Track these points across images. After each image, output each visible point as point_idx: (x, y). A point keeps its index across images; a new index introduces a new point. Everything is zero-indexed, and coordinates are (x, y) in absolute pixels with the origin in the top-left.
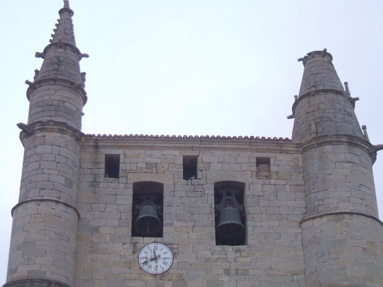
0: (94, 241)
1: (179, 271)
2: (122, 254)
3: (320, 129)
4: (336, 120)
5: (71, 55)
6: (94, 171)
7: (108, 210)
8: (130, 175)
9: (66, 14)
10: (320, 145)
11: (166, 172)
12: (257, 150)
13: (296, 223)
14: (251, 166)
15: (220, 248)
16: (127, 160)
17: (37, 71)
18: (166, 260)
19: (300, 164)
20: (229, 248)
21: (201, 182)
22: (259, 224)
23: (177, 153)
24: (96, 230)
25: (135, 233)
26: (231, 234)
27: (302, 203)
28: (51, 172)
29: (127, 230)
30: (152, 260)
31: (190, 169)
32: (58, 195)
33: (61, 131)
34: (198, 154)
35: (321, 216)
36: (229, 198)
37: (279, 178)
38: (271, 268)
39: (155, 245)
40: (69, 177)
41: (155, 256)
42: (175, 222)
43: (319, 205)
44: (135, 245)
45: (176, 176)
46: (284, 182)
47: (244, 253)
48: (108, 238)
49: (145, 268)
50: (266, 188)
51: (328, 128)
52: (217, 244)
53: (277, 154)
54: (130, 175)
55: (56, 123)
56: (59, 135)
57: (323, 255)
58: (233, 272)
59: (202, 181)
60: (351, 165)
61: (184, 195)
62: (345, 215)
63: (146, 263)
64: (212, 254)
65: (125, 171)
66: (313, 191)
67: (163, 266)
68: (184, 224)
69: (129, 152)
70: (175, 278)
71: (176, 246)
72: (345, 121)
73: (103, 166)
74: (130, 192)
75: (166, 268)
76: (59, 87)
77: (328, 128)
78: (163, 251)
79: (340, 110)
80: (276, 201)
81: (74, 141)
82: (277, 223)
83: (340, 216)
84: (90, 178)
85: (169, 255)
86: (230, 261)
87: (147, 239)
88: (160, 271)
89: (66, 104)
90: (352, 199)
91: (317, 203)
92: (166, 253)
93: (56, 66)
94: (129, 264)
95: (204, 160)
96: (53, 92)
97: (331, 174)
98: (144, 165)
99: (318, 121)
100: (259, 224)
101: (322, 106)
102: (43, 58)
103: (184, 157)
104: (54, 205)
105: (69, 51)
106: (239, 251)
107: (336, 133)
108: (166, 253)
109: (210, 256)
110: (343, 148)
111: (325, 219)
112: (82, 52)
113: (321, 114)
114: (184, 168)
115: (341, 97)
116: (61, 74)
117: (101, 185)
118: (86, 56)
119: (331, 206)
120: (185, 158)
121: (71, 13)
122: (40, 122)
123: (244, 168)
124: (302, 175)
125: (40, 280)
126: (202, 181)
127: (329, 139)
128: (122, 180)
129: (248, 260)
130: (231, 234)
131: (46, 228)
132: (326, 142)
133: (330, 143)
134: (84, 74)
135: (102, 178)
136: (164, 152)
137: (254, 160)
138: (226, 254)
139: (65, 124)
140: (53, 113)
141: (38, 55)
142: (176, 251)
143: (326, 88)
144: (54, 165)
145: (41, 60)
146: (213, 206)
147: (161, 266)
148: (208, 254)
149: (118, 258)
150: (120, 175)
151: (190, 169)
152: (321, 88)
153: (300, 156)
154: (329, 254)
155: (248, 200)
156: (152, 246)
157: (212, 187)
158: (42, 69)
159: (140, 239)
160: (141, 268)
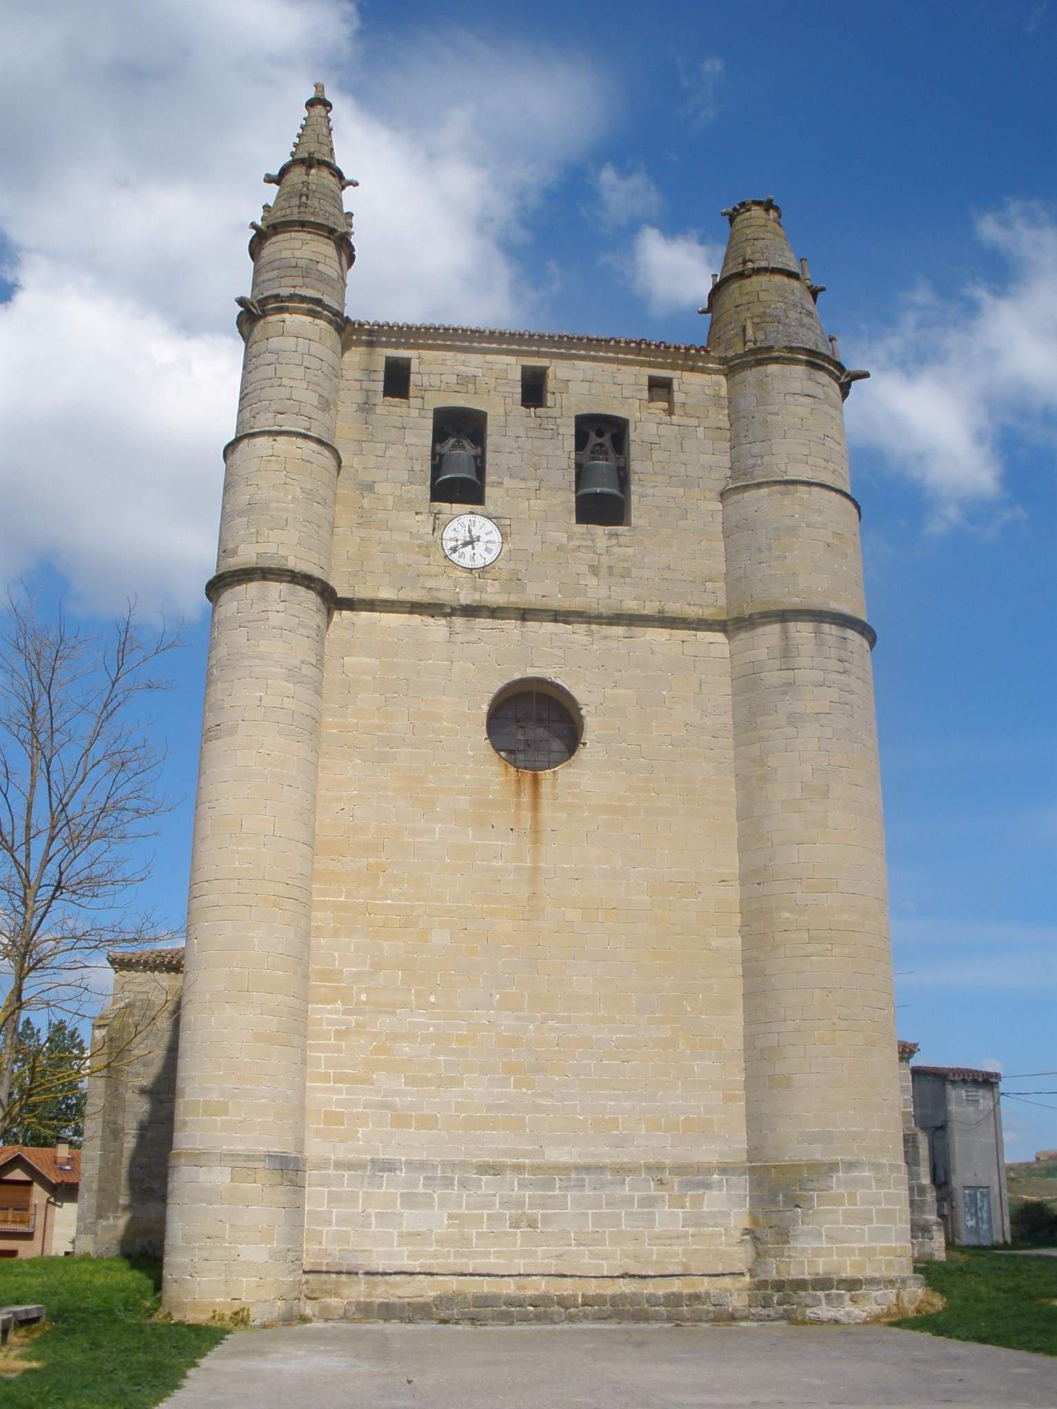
0: (366, 506)
1: (511, 565)
2: (414, 530)
3: (760, 336)
4: (787, 321)
5: (332, 181)
6: (365, 385)
7: (390, 452)
8: (428, 395)
9: (319, 109)
10: (760, 363)
11: (492, 392)
13: (713, 494)
14: (641, 390)
15: (583, 528)
16: (423, 368)
17: (266, 207)
18: (489, 545)
20: (600, 530)
21: (551, 412)
22: (650, 491)
23: (511, 360)
24: (369, 487)
25: (435, 498)
26: (602, 506)
27: (725, 460)
28: (292, 383)
29: (424, 490)
30: (465, 544)
31: (534, 390)
32: (307, 425)
33: (311, 313)
34: (547, 364)
35: (759, 485)
36: (600, 441)
37: (686, 415)
38: (669, 568)
39: (471, 517)
40: (325, 393)
41: (471, 537)
42: (506, 480)
43: (755, 465)
44: (436, 516)
45: (509, 401)
46: (695, 422)
47: (622, 540)
49: (454, 557)
50: (664, 430)
51: (774, 335)
52: (579, 521)
53: (685, 373)
54: (428, 395)
55: (303, 299)
56: (309, 319)
57: (760, 550)
59: (555, 412)
60: (810, 400)
61: (522, 433)
62: (799, 487)
63: (454, 550)
64: (570, 538)
65: (421, 387)
66: (744, 441)
67: (485, 554)
68: (523, 485)
70: (504, 576)
72: (803, 325)
73: (381, 376)
74: (429, 423)
75: (490, 558)
76: (309, 236)
77: (774, 335)
78: (485, 529)
79: (795, 305)
80: (681, 454)
81: (333, 331)
82: (681, 491)
83: (791, 487)
84: (360, 399)
85: (496, 536)
86: (599, 552)
87: (456, 507)
88: (479, 563)
89: (321, 267)
90: (811, 460)
91: (751, 461)
92: (491, 532)
93: (304, 199)
95: (559, 375)
96: (298, 245)
97: (777, 414)
98: (454, 379)
99: (757, 320)
100: (650, 491)
101: (764, 296)
102: (278, 183)
103: (524, 368)
104: (299, 441)
105: (325, 173)
107: (786, 344)
108: (491, 532)
109: (565, 541)
110: (800, 369)
111: (764, 491)
112: (347, 177)
113: (762, 310)
114: (523, 386)
115: (795, 283)
116: (313, 214)
117: (378, 410)
118: (356, 184)
119: (775, 468)
120: (525, 369)
121: (327, 105)
122: (277, 297)
123: (626, 393)
124: (726, 411)
125: (279, 569)
126: (555, 412)
127: (776, 354)
129: (630, 551)
130: (602, 506)
131: (288, 480)
132: (770, 358)
133: (777, 360)
134: (350, 215)
135: (379, 398)
136: (489, 358)
137: (645, 381)
138: (593, 540)
139: (318, 302)
140: (299, 281)
141: (269, 179)
142: (507, 529)
143: (772, 265)
144: (300, 372)
145: (275, 188)
146: (573, 455)
147: (480, 556)
148: (562, 537)
149: (408, 539)
150: (411, 394)
151: (534, 390)
152: (763, 264)
153: (722, 379)
155: (634, 450)
156: (466, 519)
157: (572, 422)
158: (276, 203)
160: (446, 556)
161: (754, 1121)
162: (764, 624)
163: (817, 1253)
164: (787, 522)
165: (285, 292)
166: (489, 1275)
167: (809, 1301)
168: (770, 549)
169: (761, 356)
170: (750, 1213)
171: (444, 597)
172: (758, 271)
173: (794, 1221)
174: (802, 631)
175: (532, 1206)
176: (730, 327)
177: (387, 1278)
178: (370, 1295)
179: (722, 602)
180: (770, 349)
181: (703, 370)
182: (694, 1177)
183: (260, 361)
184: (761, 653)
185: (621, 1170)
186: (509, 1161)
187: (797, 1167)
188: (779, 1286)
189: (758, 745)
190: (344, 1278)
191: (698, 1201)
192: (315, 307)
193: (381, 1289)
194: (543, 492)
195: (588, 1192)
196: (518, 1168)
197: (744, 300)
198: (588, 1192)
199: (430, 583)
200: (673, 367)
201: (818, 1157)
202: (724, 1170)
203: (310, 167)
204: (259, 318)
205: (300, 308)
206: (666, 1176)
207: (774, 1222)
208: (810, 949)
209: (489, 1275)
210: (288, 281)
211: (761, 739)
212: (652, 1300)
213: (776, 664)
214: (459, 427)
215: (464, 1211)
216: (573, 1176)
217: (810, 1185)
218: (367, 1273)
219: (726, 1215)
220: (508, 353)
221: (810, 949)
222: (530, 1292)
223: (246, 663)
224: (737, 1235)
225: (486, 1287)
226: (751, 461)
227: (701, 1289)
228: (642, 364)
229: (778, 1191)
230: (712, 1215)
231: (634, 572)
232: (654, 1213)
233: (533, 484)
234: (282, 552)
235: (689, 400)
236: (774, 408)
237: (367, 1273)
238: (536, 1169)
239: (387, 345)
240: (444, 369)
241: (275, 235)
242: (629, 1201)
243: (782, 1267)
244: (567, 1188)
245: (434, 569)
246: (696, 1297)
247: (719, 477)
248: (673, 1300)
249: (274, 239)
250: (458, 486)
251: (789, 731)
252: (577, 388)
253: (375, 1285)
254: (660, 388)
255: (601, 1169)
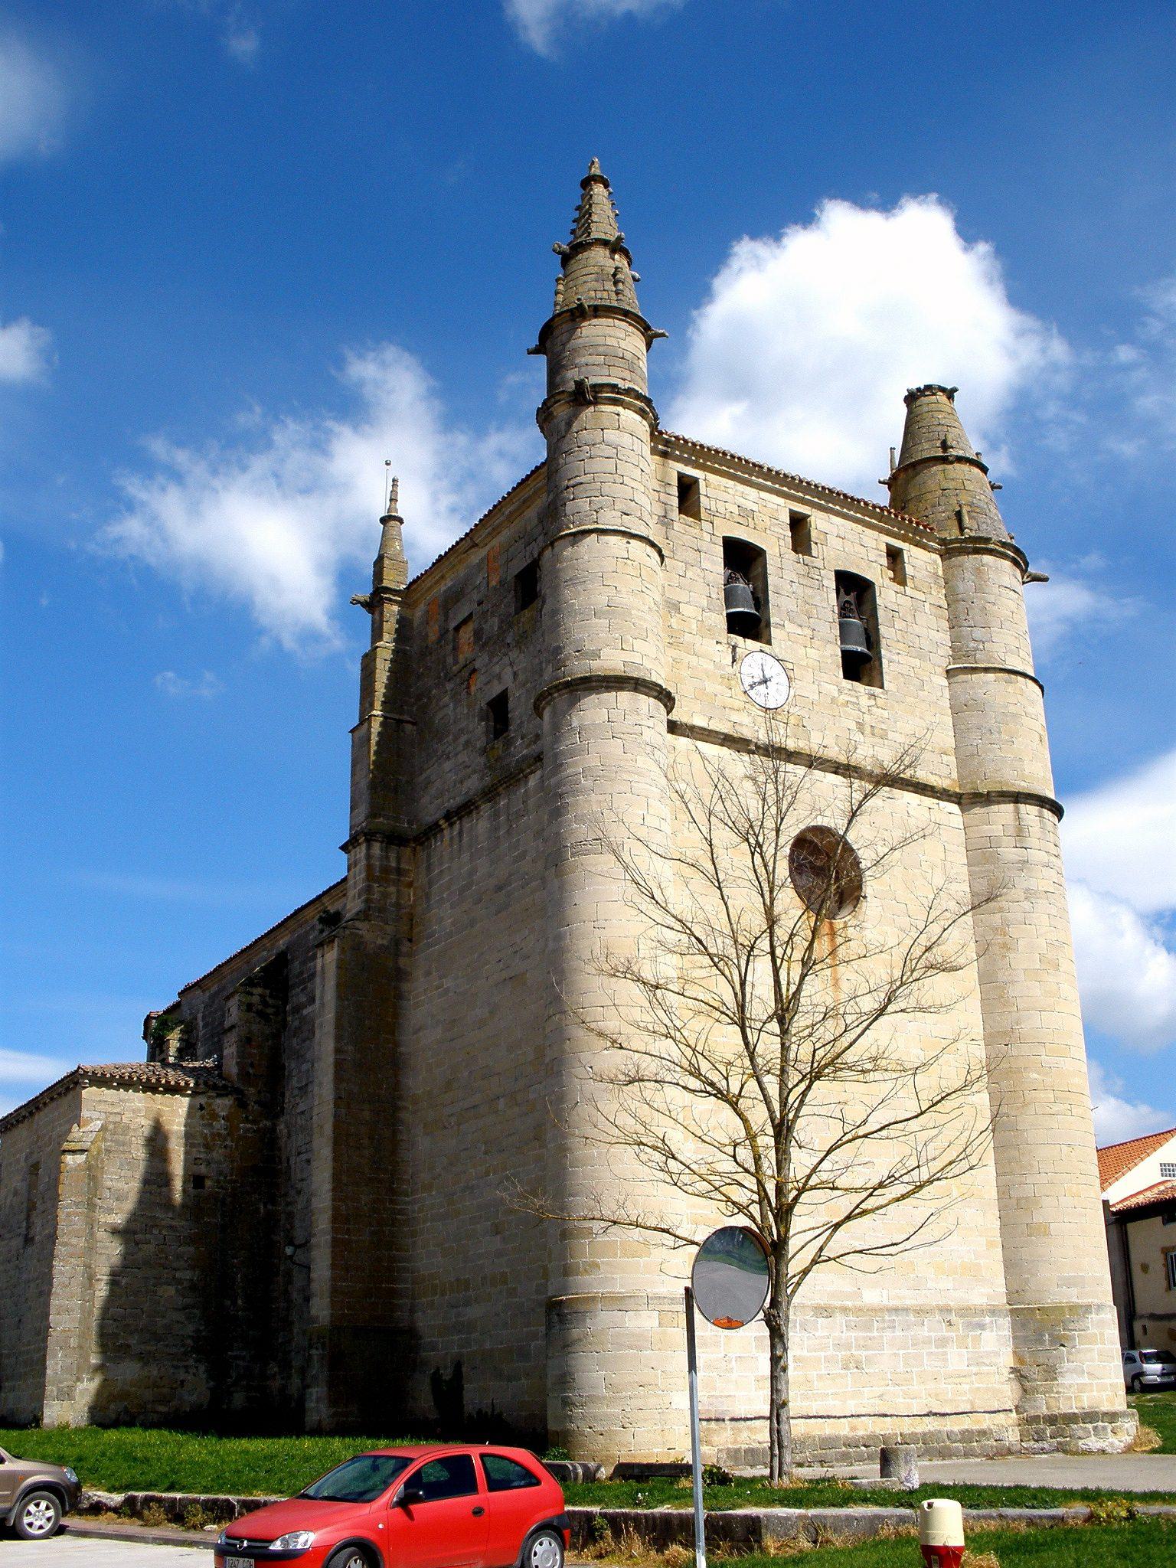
10: (977, 551)
12: (888, 533)
19: (940, 573)
22: (895, 657)
26: (860, 666)
27: (945, 638)
30: (760, 683)
33: (642, 413)
35: (986, 670)
37: (916, 588)
46: (922, 597)
47: (880, 702)
48: (694, 626)
50: (901, 599)
55: (639, 396)
56: (638, 418)
58: (868, 730)
62: (1019, 678)
69: (711, 477)
71: (790, 666)
73: (675, 491)
76: (631, 329)
87: (751, 644)
91: (972, 644)
94: (727, 681)
96: (622, 335)
98: (736, 510)
100: (895, 657)
101: (969, 486)
106: (873, 696)
111: (991, 676)
117: (676, 526)
122: (615, 386)
126: (818, 563)
127: (991, 546)
128: (706, 526)
129: (885, 714)
130: (860, 666)
133: (991, 552)
135: (675, 514)
136: (763, 494)
140: (627, 375)
142: (791, 673)
152: (961, 453)
154: (1000, 732)
159: (739, 640)
161: (1011, 1265)
162: (999, 803)
163: (1082, 1388)
164: (1012, 709)
165: (622, 385)
166: (829, 1417)
167: (1080, 1433)
168: (1000, 732)
169: (979, 546)
170: (1015, 1352)
171: (747, 733)
172: (960, 459)
173: (1061, 1358)
174: (1030, 811)
175: (858, 1347)
176: (941, 509)
177: (749, 1423)
178: (735, 1442)
179: (955, 775)
180: (988, 540)
181: (925, 547)
182: (972, 1316)
183: (595, 451)
184: (996, 830)
185: (921, 1311)
186: (838, 1303)
187: (1058, 1309)
188: (1052, 1420)
189: (998, 915)
190: (713, 1424)
191: (977, 1340)
192: (647, 408)
193: (744, 1435)
194: (816, 642)
195: (898, 1333)
196: (845, 1310)
197: (951, 485)
198: (898, 1333)
199: (735, 717)
200: (904, 539)
201: (1075, 1300)
202: (993, 1312)
203: (613, 251)
204: (590, 403)
205: (634, 405)
206: (954, 1318)
207: (1041, 1361)
208: (1056, 1108)
209: (829, 1417)
210: (614, 371)
211: (1001, 910)
212: (949, 1435)
213: (1012, 841)
214: (742, 558)
215: (805, 1353)
216: (887, 1318)
217: (1071, 1326)
218: (732, 1419)
219: (997, 1354)
220: (779, 493)
221: (1056, 1108)
222: (861, 1433)
223: (625, 776)
224: (1006, 1372)
225: (828, 1428)
226: (972, 644)
227: (984, 1426)
228: (881, 530)
229: (1038, 1330)
230: (988, 1354)
231: (891, 735)
232: (945, 1353)
233: (808, 632)
234: (648, 664)
235: (917, 574)
236: (992, 599)
237: (732, 1419)
238: (859, 1311)
239: (678, 459)
240: (727, 497)
241: (596, 317)
242: (927, 1341)
243: (1052, 1403)
244: (883, 1328)
245: (737, 704)
246: (983, 1433)
247: (942, 657)
248: (967, 1436)
249: (595, 321)
250: (749, 624)
251: (1027, 905)
252: (832, 540)
253: (739, 1430)
254: (894, 556)
255: (906, 1310)
